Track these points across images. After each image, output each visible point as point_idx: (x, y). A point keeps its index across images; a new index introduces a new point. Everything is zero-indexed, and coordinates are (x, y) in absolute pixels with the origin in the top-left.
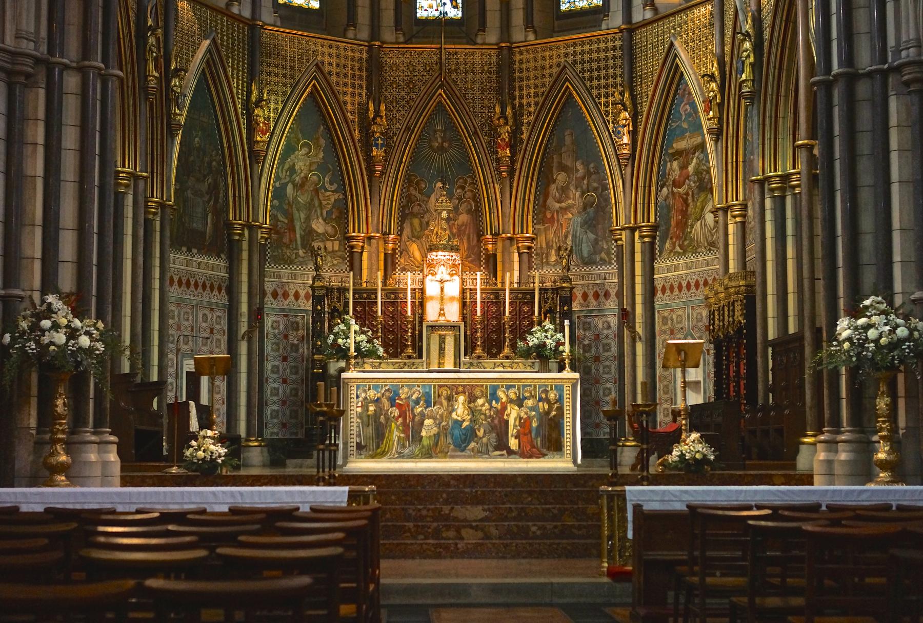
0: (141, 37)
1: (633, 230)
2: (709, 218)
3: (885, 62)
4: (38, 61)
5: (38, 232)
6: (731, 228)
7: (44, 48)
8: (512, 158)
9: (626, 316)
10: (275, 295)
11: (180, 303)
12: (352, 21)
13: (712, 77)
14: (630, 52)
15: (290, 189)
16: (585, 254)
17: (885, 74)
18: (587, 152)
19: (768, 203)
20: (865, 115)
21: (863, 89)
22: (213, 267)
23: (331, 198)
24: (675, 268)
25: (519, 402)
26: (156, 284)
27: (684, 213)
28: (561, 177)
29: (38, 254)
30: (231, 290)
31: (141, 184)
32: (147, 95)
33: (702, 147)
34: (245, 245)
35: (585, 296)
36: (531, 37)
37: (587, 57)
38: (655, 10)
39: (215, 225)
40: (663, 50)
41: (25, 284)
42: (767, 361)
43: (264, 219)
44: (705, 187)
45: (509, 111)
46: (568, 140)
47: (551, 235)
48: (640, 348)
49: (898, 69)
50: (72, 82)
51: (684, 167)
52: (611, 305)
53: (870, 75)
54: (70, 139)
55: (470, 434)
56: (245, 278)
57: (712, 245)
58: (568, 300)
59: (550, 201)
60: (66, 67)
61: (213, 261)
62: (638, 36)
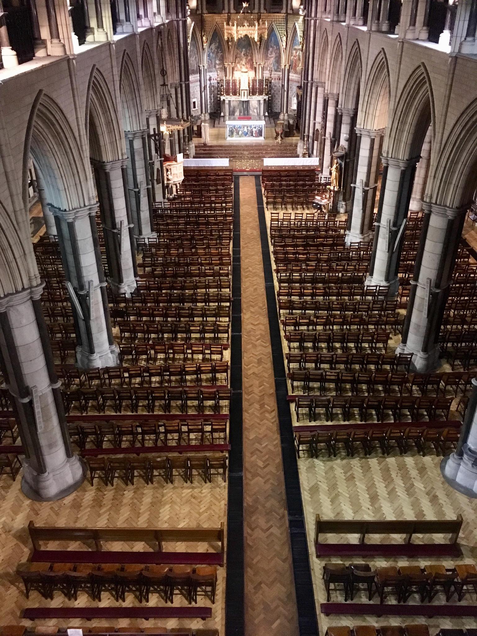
9: (283, 86)
12: (224, 9)
18: (277, 44)
21: (309, 85)
23: (220, 54)
28: (271, 49)
44: (299, 59)
48: (285, 93)
50: (184, 85)
52: (281, 82)
55: (247, 133)
62: (289, 16)
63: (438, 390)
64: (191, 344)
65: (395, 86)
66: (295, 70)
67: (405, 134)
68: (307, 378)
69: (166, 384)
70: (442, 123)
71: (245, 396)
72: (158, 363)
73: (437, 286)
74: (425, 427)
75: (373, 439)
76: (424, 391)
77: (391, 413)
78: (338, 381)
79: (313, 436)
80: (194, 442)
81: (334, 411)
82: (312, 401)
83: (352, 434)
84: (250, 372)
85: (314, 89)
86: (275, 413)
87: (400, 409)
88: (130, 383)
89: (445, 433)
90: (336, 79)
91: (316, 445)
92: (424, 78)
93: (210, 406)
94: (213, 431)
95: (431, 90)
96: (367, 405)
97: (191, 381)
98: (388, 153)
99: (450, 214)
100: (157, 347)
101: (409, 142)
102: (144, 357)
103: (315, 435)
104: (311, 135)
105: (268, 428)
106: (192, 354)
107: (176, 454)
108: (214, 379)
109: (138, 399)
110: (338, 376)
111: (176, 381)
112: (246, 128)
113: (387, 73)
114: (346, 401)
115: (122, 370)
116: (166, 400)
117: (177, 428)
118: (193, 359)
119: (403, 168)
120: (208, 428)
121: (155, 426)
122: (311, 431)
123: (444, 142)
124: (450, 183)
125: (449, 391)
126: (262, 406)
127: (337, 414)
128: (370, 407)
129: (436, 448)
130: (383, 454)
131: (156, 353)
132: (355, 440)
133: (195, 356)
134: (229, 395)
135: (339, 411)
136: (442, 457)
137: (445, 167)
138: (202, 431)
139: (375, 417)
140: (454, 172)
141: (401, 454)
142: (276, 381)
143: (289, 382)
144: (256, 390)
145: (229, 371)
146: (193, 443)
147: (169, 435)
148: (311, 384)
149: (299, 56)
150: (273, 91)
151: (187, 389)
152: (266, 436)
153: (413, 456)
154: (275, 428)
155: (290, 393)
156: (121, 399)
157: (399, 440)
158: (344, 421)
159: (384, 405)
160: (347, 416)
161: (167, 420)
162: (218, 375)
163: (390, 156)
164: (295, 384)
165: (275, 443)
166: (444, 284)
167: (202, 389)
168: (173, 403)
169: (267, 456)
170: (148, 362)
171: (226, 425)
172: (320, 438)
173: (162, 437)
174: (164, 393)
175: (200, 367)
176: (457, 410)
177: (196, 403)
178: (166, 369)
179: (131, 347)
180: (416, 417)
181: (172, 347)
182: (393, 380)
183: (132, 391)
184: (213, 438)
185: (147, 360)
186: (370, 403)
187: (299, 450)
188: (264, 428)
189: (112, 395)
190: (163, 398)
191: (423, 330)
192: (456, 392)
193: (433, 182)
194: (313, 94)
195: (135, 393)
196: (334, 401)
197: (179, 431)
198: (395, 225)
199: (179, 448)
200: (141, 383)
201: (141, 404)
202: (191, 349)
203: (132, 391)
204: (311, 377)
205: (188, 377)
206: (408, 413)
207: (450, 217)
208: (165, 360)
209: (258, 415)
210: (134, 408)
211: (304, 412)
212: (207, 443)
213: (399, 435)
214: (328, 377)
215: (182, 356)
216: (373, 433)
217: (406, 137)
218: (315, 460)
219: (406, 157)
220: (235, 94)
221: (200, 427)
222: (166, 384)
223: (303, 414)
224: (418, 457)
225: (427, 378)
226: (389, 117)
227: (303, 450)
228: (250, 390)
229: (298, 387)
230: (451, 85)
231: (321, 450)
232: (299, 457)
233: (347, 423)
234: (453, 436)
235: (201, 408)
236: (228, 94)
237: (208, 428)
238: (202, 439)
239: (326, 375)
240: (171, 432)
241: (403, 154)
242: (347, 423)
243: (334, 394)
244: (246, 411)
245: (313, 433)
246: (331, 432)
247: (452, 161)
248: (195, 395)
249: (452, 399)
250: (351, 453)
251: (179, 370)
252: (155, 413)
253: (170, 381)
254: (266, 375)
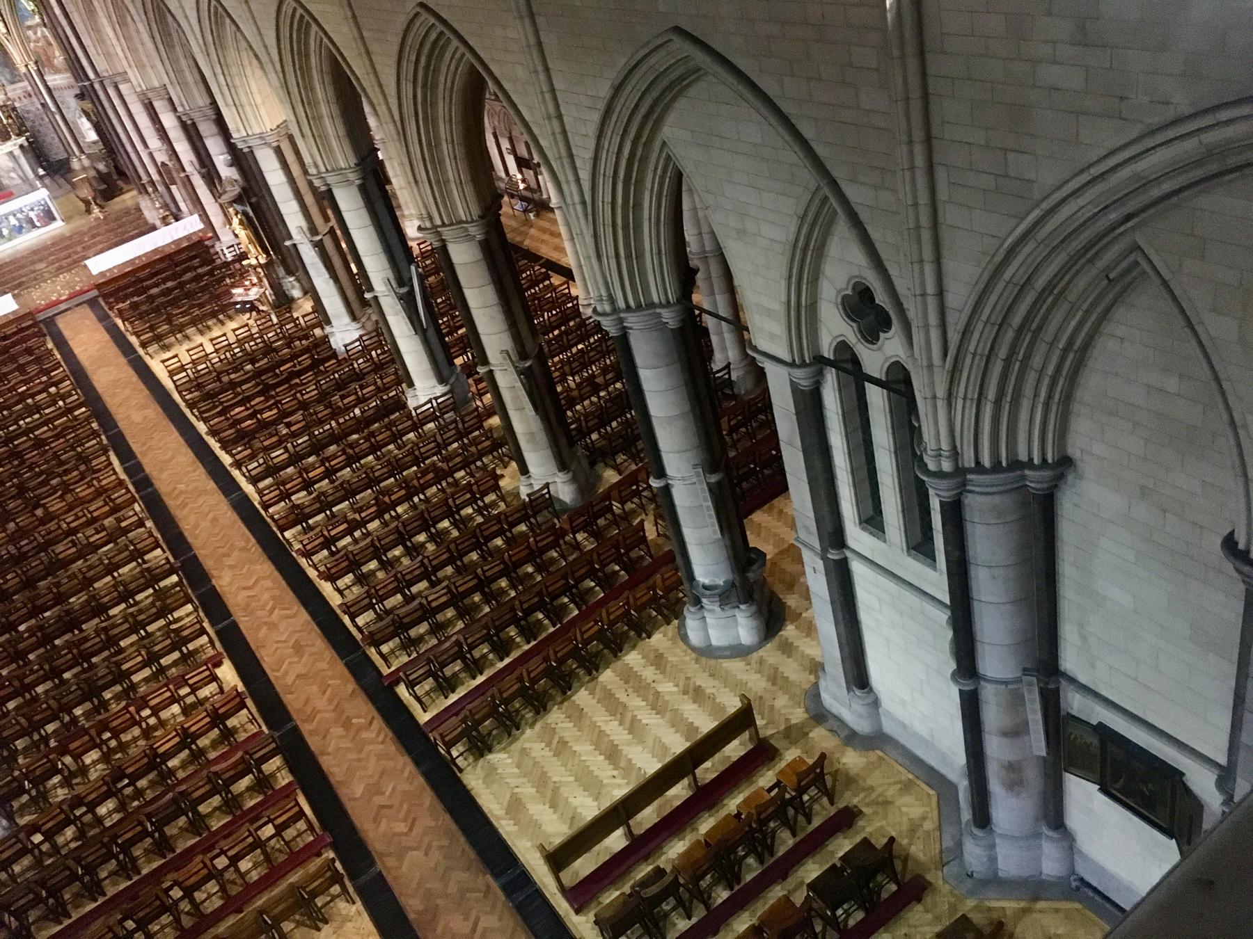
9: (44, 105)
21: (97, 86)
25: (32, 210)
48: (58, 117)
52: (35, 99)
63: (616, 521)
64: (142, 698)
65: (261, 44)
66: (52, 66)
67: (327, 122)
68: (398, 627)
69: (136, 803)
70: (377, 88)
71: (305, 728)
72: (93, 775)
73: (523, 356)
74: (626, 593)
75: (561, 662)
76: (596, 534)
77: (566, 600)
78: (455, 599)
79: (464, 721)
80: (254, 873)
81: (477, 653)
82: (429, 661)
83: (525, 674)
84: (289, 680)
86: (378, 722)
87: (575, 586)
88: (56, 849)
89: (659, 582)
90: (145, 59)
91: (478, 731)
92: (302, 16)
93: (248, 789)
94: (280, 829)
95: (326, 33)
96: (523, 611)
97: (183, 765)
98: (316, 166)
99: (476, 231)
100: (73, 746)
101: (342, 131)
102: (56, 779)
103: (466, 717)
104: (155, 177)
105: (380, 757)
106: (155, 712)
107: (231, 920)
108: (227, 734)
109: (91, 870)
110: (450, 591)
111: (152, 784)
112: (11, 218)
113: (234, 28)
114: (486, 627)
115: (22, 836)
116: (151, 835)
117: (205, 871)
118: (162, 723)
119: (358, 182)
120: (269, 830)
121: (158, 897)
122: (456, 714)
123: (397, 117)
124: (447, 182)
125: (633, 511)
126: (347, 724)
127: (484, 656)
128: (529, 612)
129: (660, 613)
130: (590, 674)
131: (77, 757)
132: (534, 681)
133: (164, 715)
134: (273, 745)
135: (485, 649)
136: (676, 622)
137: (424, 159)
138: (258, 844)
139: (546, 622)
140: (442, 162)
141: (616, 656)
142: (346, 664)
143: (372, 652)
144: (321, 703)
145: (249, 702)
146: (255, 876)
147: (196, 894)
148: (413, 633)
149: (45, 37)
150: (28, 124)
151: (183, 787)
152: (383, 773)
153: (634, 647)
154: (391, 747)
155: (385, 671)
156: (55, 892)
157: (600, 636)
158: (502, 659)
159: (549, 595)
160: (502, 649)
161: (177, 869)
162: (232, 722)
163: (323, 169)
164: (385, 648)
165: (406, 774)
166: (530, 346)
167: (214, 769)
168: (171, 830)
169: (405, 807)
170: (70, 786)
171: (297, 804)
172: (477, 717)
173: (185, 906)
174: (141, 823)
175: (185, 730)
176: (659, 535)
177: (216, 800)
178: (118, 774)
179: (15, 779)
180: (606, 581)
181: (103, 726)
182: (540, 545)
183: (70, 863)
184: (287, 843)
185: (67, 783)
186: (525, 606)
187: (453, 760)
188: (373, 759)
189: (31, 896)
190: (145, 834)
191: (542, 437)
192: (642, 507)
193: (419, 189)
194: (117, 102)
195: (78, 861)
196: (466, 639)
197: (214, 874)
198: (401, 283)
199: (232, 904)
200: (81, 835)
201: (103, 875)
202: (147, 706)
203: (70, 863)
204: (406, 620)
205: (173, 763)
206: (593, 584)
207: (479, 237)
208: (106, 758)
209: (349, 745)
210: (95, 889)
211: (427, 688)
212: (282, 858)
213: (596, 628)
214: (434, 604)
215: (136, 731)
216: (556, 653)
217: (333, 128)
218: (490, 757)
219: (353, 161)
221: (250, 840)
222: (136, 803)
223: (427, 693)
224: (641, 644)
225: (589, 511)
226: (282, 102)
227: (461, 754)
228: (308, 710)
229: (392, 652)
230: (354, 16)
231: (490, 734)
232: (461, 771)
233: (507, 661)
234: (673, 579)
235: (231, 804)
237: (269, 830)
238: (268, 858)
239: (429, 603)
240: (198, 886)
241: (344, 157)
242: (507, 661)
243: (460, 625)
244: (323, 754)
245: (461, 716)
246: (489, 693)
247: (429, 144)
248: (208, 787)
249: (642, 521)
250: (540, 706)
251: (146, 760)
252: (144, 872)
253: (139, 793)
254: (324, 665)
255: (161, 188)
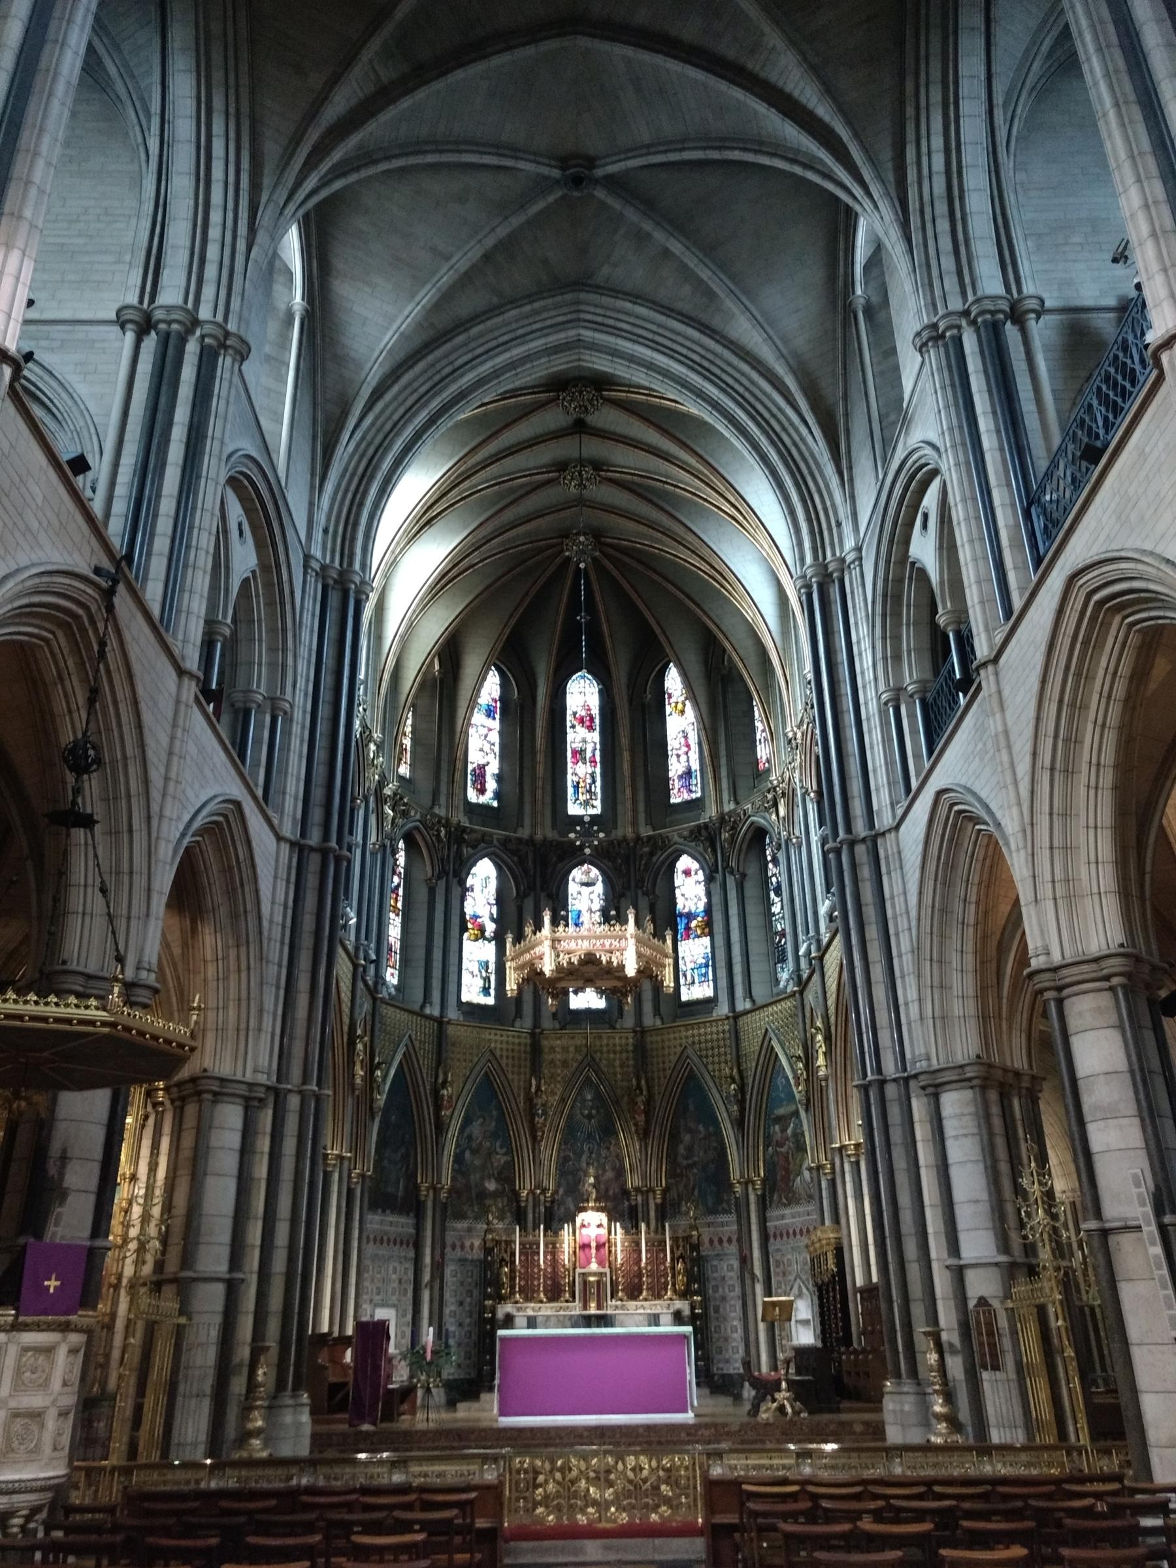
0: (352, 1044)
1: (746, 1184)
2: (807, 1174)
3: (905, 1070)
4: (268, 1088)
5: (260, 1224)
6: (824, 1184)
7: (274, 1078)
8: (648, 1122)
10: (454, 1247)
11: (375, 1257)
13: (799, 1058)
14: (736, 1033)
15: (467, 1154)
16: (710, 1204)
17: (906, 1080)
19: (847, 1167)
20: (895, 1113)
21: (891, 1091)
22: (402, 1224)
24: (783, 1217)
26: (355, 1244)
27: (787, 1170)
29: (258, 1242)
30: (418, 1246)
31: (346, 1163)
32: (353, 1091)
33: (796, 1114)
34: (430, 1204)
35: (711, 1242)
36: (658, 1022)
37: (703, 1038)
38: (753, 1001)
39: (406, 1188)
40: (760, 1033)
41: (247, 1268)
42: (856, 1306)
43: (447, 1181)
44: (801, 1148)
45: (643, 1082)
46: (691, 1107)
47: (681, 1188)
49: (916, 1076)
50: (294, 1101)
51: (784, 1130)
53: (895, 1080)
54: (289, 1146)
56: (429, 1233)
57: (810, 1197)
58: (696, 1247)
59: (680, 1159)
60: (290, 1091)
61: (402, 1220)
62: (741, 1021)
85: (919, 1106)
220: (554, 1294)
236: (529, 1295)
255: (956, 1366)
